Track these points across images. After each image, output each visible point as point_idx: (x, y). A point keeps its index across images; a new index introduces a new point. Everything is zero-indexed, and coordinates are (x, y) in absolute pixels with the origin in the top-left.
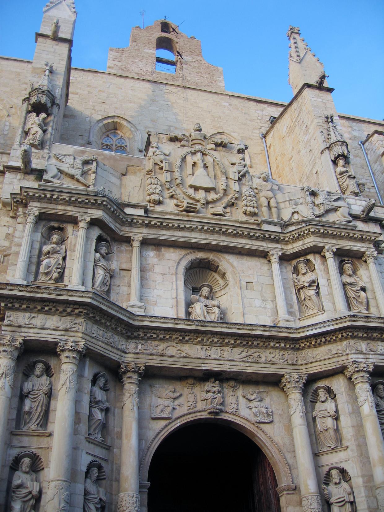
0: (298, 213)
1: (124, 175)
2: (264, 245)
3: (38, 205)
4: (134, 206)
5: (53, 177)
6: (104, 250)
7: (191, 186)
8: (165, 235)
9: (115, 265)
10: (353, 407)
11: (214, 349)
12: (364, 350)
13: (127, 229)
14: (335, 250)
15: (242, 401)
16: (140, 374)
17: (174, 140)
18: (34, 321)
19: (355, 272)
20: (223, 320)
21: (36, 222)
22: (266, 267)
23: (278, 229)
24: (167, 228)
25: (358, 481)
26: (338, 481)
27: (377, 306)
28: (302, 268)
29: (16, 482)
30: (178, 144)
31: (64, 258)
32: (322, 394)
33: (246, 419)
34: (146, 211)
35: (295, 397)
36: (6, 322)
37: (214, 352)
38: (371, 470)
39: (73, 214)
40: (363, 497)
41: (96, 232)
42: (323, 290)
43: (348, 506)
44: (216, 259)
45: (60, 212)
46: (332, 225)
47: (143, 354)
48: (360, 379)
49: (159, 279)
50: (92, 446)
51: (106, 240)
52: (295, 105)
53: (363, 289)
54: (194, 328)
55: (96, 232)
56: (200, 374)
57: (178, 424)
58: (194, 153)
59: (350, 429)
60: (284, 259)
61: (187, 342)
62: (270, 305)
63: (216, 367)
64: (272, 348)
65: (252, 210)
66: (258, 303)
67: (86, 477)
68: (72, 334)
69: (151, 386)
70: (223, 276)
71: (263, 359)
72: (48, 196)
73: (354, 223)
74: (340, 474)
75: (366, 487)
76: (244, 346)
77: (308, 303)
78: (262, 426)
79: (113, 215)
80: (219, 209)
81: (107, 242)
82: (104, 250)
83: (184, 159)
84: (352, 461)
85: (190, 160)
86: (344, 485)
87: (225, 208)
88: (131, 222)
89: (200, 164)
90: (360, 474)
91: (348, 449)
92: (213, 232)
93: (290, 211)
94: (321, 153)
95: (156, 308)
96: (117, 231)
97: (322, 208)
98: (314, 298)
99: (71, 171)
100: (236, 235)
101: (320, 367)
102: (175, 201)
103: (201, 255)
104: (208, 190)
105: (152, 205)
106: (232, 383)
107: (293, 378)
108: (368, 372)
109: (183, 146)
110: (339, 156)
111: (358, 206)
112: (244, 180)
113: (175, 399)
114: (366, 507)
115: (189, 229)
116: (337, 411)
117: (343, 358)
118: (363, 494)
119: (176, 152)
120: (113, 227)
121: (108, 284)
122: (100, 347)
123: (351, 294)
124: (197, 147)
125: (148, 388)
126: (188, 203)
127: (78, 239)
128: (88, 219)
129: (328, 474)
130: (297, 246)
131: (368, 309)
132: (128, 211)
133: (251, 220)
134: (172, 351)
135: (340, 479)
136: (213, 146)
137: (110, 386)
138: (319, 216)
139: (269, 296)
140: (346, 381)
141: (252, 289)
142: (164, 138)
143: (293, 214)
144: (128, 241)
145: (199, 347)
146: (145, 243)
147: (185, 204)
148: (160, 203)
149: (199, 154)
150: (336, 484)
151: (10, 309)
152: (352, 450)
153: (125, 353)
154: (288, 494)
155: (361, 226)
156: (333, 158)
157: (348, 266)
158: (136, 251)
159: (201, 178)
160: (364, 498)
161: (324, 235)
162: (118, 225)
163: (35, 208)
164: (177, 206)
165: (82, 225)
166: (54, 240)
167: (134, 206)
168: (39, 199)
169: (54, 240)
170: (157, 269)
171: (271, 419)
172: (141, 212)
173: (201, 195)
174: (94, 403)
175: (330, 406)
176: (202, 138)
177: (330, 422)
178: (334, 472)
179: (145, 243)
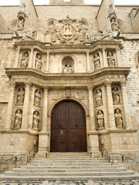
0: (96, 39)
1: (45, 35)
2: (84, 50)
3: (20, 46)
4: (48, 43)
5: (25, 38)
6: (39, 57)
7: (64, 35)
8: (56, 51)
9: (43, 61)
11: (68, 81)
12: (110, 77)
13: (45, 50)
14: (105, 48)
15: (76, 94)
16: (48, 89)
17: (60, 21)
18: (18, 77)
19: (112, 55)
20: (73, 73)
21: (20, 52)
22: (85, 57)
23: (90, 45)
24: (56, 48)
25: (105, 113)
27: (118, 65)
28: (96, 55)
29: (16, 116)
30: (61, 23)
31: (28, 60)
33: (77, 99)
34: (51, 45)
35: (91, 92)
36: (12, 78)
37: (68, 82)
38: (108, 110)
39: (29, 48)
41: (36, 52)
42: (101, 61)
43: (102, 120)
44: (71, 56)
45: (26, 48)
46: (107, 41)
47: (49, 83)
49: (55, 63)
50: (35, 107)
51: (40, 54)
52: (102, 4)
53: (114, 60)
54: (61, 75)
55: (36, 52)
56: (65, 88)
57: (59, 101)
58: (66, 25)
59: (105, 100)
60: (90, 54)
61: (60, 80)
62: (85, 68)
63: (68, 85)
64: (84, 79)
65: (82, 40)
66: (82, 67)
67: (34, 114)
68: (27, 80)
69: (52, 92)
70: (73, 60)
71: (81, 83)
72: (22, 43)
73: (114, 40)
76: (76, 79)
77: (96, 66)
78: (81, 100)
79: (40, 46)
80: (73, 41)
81: (40, 54)
82: (39, 57)
83: (63, 27)
85: (65, 27)
87: (74, 40)
88: (46, 48)
89: (68, 28)
92: (69, 48)
93: (94, 38)
94: (107, 18)
95: (53, 71)
96: (42, 51)
97: (103, 36)
98: (98, 64)
99: (29, 36)
100: (76, 48)
102: (60, 41)
103: (66, 55)
104: (69, 36)
106: (74, 89)
107: (90, 87)
108: (110, 84)
109: (63, 23)
110: (112, 18)
111: (115, 34)
112: (81, 31)
113: (58, 95)
115: (63, 48)
116: (102, 95)
117: (103, 80)
119: (60, 25)
120: (41, 50)
121: (40, 66)
122: (36, 82)
123: (110, 62)
124: (67, 23)
125: (51, 92)
127: (32, 55)
128: (33, 49)
129: (98, 112)
130: (94, 49)
131: (115, 65)
132: (46, 45)
133: (82, 43)
134: (56, 82)
136: (72, 22)
137: (41, 92)
138: (102, 39)
139: (85, 65)
141: (81, 63)
143: (95, 40)
144: (46, 54)
145: (64, 81)
146: (50, 54)
147: (62, 41)
148: (55, 41)
149: (68, 25)
150: (100, 114)
151: (12, 75)
153: (44, 83)
155: (116, 40)
156: (111, 19)
157: (110, 53)
158: (48, 56)
159: (68, 32)
161: (102, 45)
162: (42, 50)
163: (19, 48)
164: (60, 42)
165: (32, 51)
166: (25, 56)
167: (48, 43)
168: (20, 45)
169: (25, 56)
170: (54, 61)
172: (50, 45)
173: (68, 37)
174: (35, 97)
176: (69, 20)
178: (99, 111)
179: (50, 54)
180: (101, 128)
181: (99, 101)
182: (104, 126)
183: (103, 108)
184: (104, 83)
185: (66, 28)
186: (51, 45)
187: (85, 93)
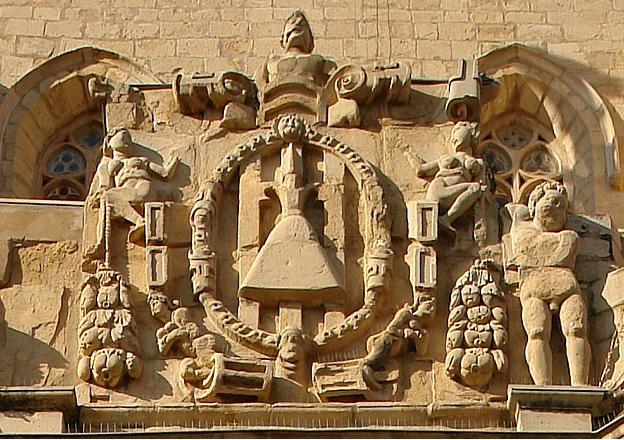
58: (268, 155)
83: (228, 187)
85: (251, 186)
104: (313, 304)
105: (101, 391)
109: (233, 127)
126: (228, 365)
142: (161, 104)
185: (269, 206)
186: (74, 416)
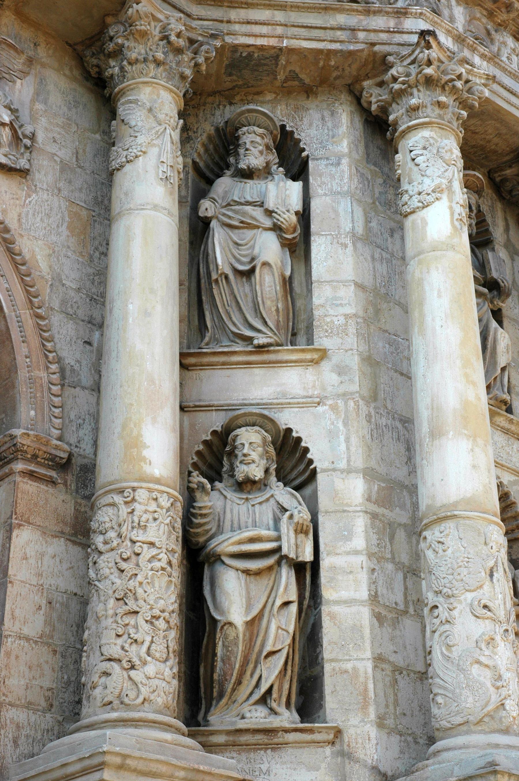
10: (368, 221)
25: (345, 486)
26: (256, 472)
32: (255, 150)
40: (356, 553)
43: (287, 577)
48: (431, 113)
59: (348, 293)
74: (271, 450)
75: (374, 516)
84: (334, 408)
86: (282, 494)
90: (359, 462)
91: (326, 365)
101: (279, 30)
114: (364, 594)
116: (304, 216)
118: (359, 542)
135: (267, 471)
140: (358, 124)
150: (246, 486)
152: (341, 370)
154: (31, 475)
160: (363, 558)
171: (23, 163)
175: (283, 194)
177: (269, 248)
180: (258, 717)
181: (268, 285)
182: (308, 697)
183: (312, 397)
184: (378, 64)
187: (40, 94)
